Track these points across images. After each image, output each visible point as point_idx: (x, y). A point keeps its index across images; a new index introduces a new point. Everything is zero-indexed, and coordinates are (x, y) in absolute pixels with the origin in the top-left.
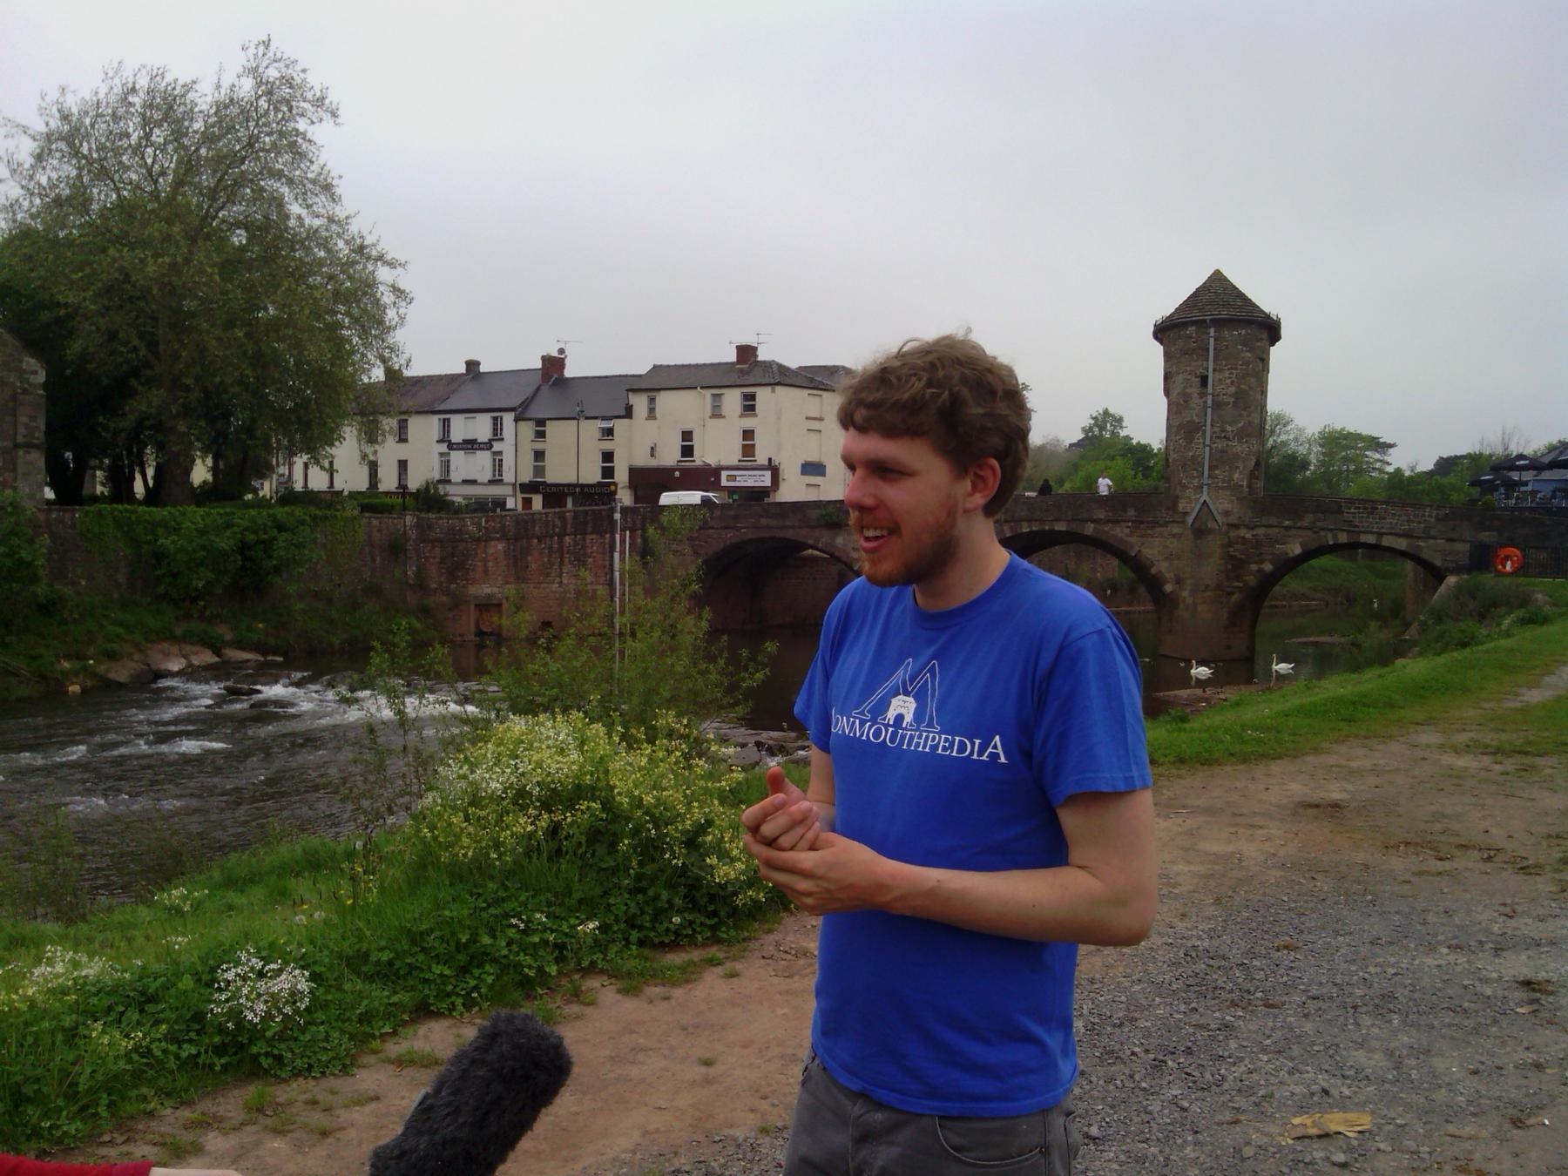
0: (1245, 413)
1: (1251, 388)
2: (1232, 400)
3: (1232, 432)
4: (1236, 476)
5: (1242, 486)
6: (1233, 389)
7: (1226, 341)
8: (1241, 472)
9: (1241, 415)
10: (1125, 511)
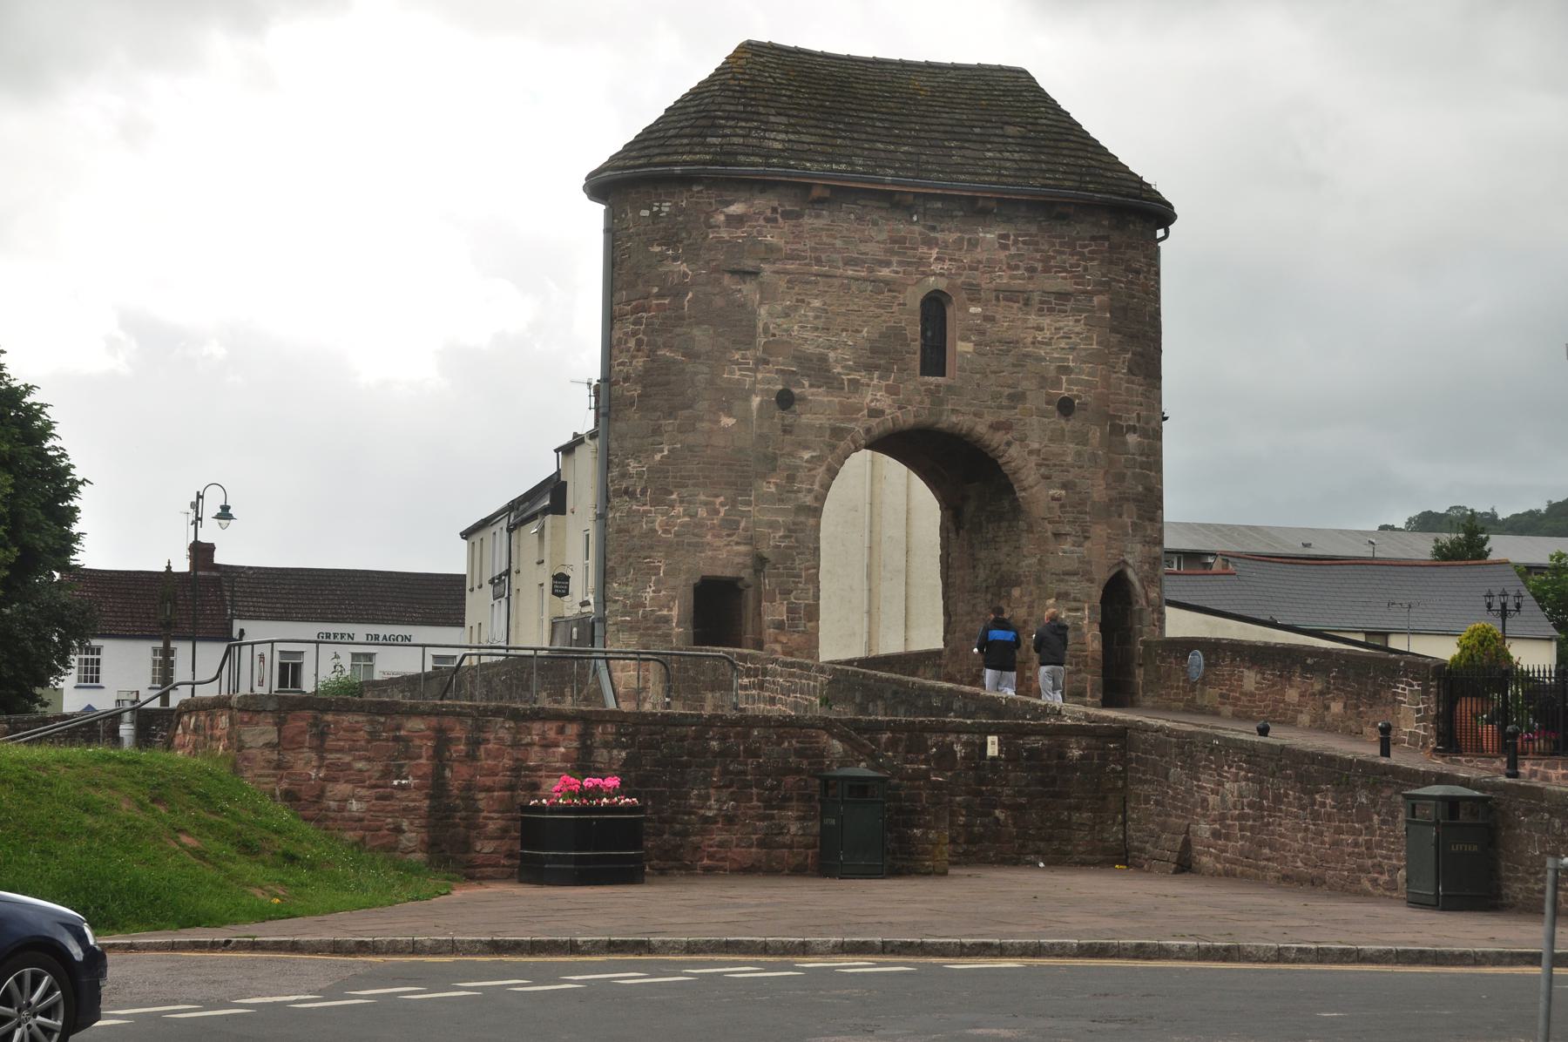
0: (669, 424)
1: (692, 355)
2: (636, 391)
3: (640, 475)
4: (649, 594)
5: (667, 620)
6: (639, 362)
7: (630, 237)
8: (658, 582)
9: (657, 431)
10: (563, 695)
